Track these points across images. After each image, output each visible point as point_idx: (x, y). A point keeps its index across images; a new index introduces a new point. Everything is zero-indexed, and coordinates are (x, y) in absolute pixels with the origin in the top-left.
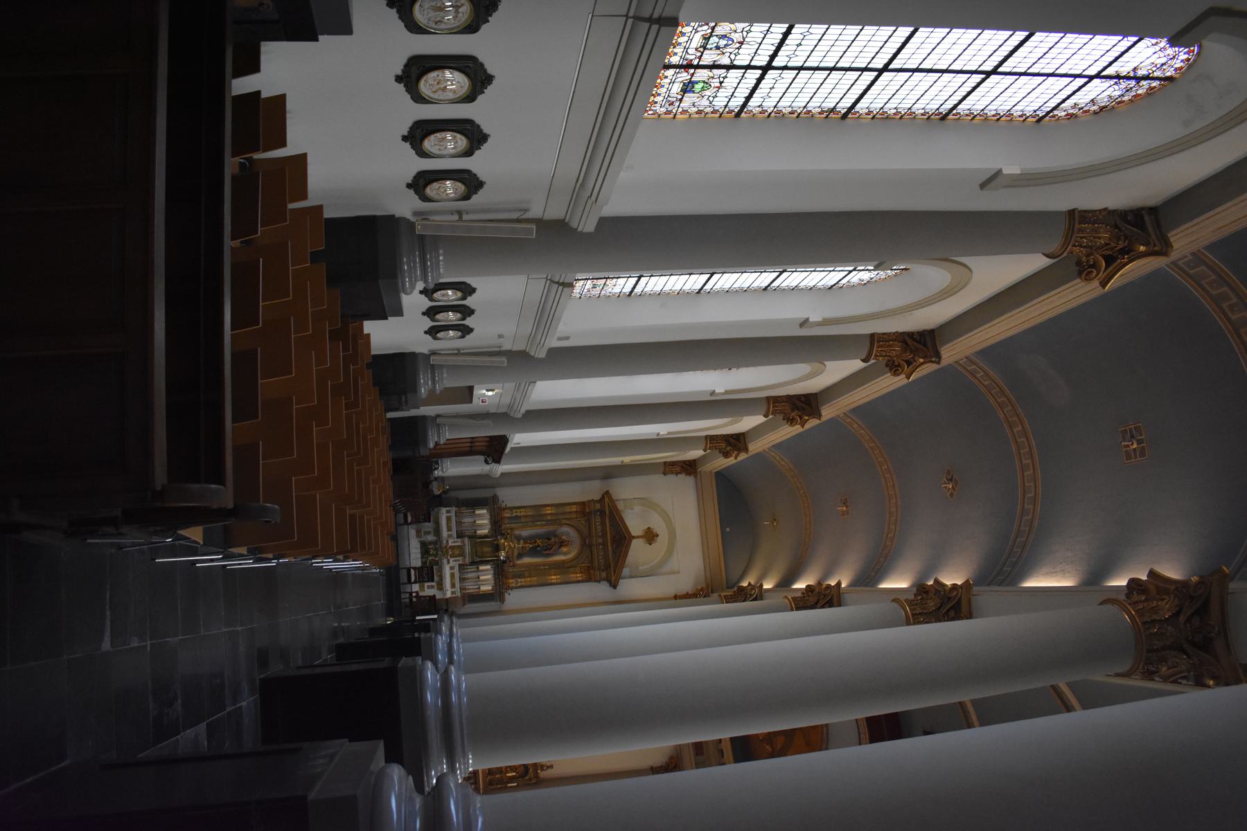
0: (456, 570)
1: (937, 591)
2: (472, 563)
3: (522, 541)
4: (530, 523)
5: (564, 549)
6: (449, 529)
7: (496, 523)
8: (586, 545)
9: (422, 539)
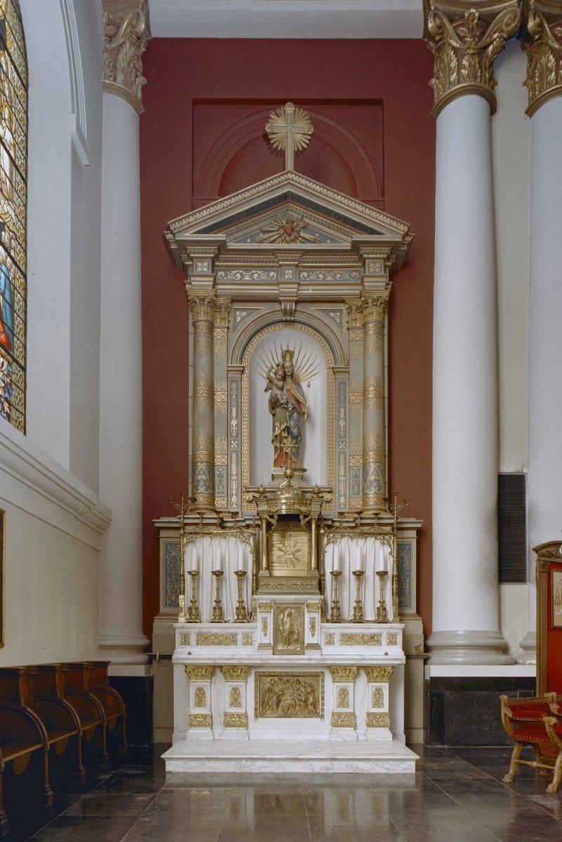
0: (336, 629)
4: (234, 444)
6: (231, 640)
9: (251, 713)
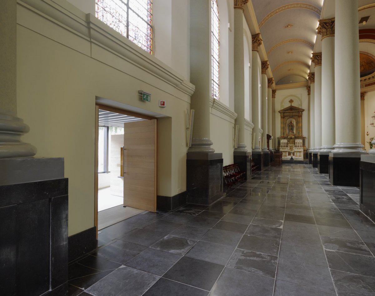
0: (296, 148)
1: (320, 29)
2: (295, 144)
3: (290, 132)
5: (293, 122)
6: (285, 149)
7: (284, 138)
8: (292, 117)
